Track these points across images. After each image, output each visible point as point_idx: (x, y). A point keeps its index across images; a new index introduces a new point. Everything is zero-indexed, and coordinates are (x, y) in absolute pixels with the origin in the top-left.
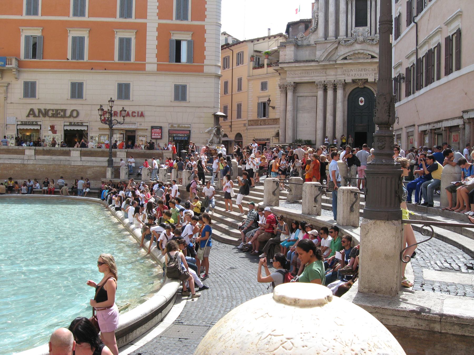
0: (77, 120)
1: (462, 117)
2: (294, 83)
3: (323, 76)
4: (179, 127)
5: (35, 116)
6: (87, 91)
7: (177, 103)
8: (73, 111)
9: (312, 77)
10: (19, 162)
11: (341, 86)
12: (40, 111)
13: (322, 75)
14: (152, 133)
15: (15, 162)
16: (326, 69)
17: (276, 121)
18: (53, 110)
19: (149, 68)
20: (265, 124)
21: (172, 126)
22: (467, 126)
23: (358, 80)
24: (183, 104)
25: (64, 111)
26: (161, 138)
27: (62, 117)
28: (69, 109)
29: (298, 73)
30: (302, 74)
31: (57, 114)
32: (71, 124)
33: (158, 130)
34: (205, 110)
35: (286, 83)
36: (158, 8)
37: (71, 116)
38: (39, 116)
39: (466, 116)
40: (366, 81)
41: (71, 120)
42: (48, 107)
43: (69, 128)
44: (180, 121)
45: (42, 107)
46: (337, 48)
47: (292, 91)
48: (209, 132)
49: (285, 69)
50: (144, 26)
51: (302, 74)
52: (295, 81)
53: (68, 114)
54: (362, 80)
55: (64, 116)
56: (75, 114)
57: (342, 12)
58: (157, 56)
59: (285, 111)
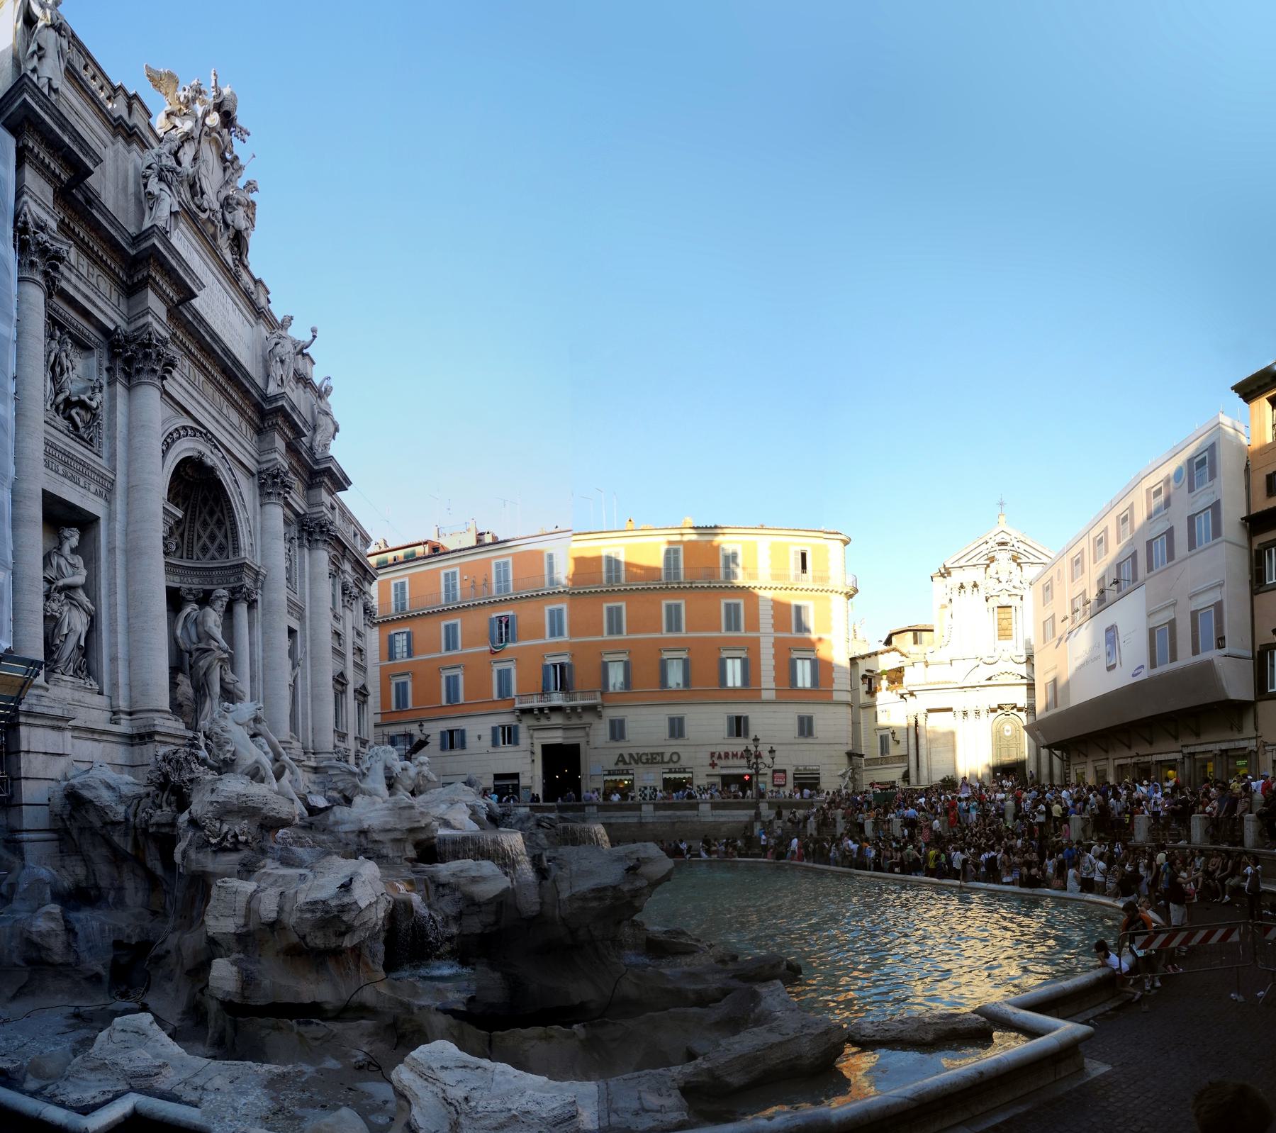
0: (677, 766)
1: (1181, 751)
4: (805, 769)
5: (625, 763)
6: (688, 728)
7: (802, 740)
8: (673, 753)
10: (635, 820)
12: (631, 755)
14: (773, 778)
15: (630, 820)
17: (903, 758)
18: (647, 754)
19: (766, 695)
20: (887, 763)
21: (797, 769)
22: (1186, 760)
24: (810, 740)
25: (662, 754)
26: (784, 785)
27: (658, 763)
28: (668, 752)
31: (653, 759)
32: (670, 772)
33: (781, 774)
34: (837, 747)
36: (773, 617)
37: (671, 760)
38: (630, 763)
39: (1186, 751)
41: (671, 765)
42: (641, 751)
43: (667, 776)
44: (806, 763)
45: (634, 751)
48: (843, 776)
50: (757, 640)
53: (666, 759)
55: (663, 762)
56: (675, 758)
58: (776, 679)
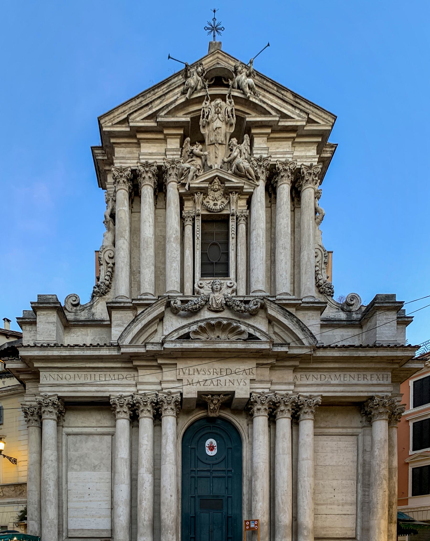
2: (59, 398)
3: (129, 385)
9: (102, 385)
11: (173, 406)
13: (125, 382)
16: (135, 369)
23: (210, 396)
29: (68, 377)
30: (77, 379)
35: (40, 398)
40: (227, 398)
46: (160, 319)
47: (55, 417)
49: (36, 365)
51: (77, 379)
52: (60, 394)
54: (219, 394)
57: (172, 239)
59: (37, 466)
